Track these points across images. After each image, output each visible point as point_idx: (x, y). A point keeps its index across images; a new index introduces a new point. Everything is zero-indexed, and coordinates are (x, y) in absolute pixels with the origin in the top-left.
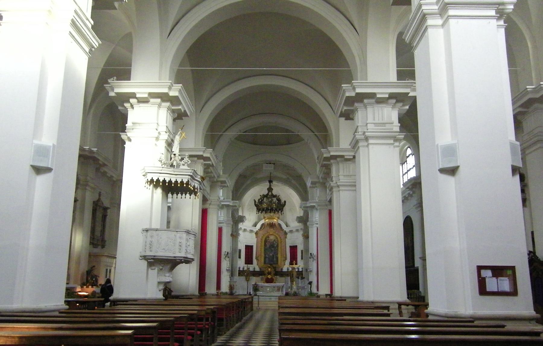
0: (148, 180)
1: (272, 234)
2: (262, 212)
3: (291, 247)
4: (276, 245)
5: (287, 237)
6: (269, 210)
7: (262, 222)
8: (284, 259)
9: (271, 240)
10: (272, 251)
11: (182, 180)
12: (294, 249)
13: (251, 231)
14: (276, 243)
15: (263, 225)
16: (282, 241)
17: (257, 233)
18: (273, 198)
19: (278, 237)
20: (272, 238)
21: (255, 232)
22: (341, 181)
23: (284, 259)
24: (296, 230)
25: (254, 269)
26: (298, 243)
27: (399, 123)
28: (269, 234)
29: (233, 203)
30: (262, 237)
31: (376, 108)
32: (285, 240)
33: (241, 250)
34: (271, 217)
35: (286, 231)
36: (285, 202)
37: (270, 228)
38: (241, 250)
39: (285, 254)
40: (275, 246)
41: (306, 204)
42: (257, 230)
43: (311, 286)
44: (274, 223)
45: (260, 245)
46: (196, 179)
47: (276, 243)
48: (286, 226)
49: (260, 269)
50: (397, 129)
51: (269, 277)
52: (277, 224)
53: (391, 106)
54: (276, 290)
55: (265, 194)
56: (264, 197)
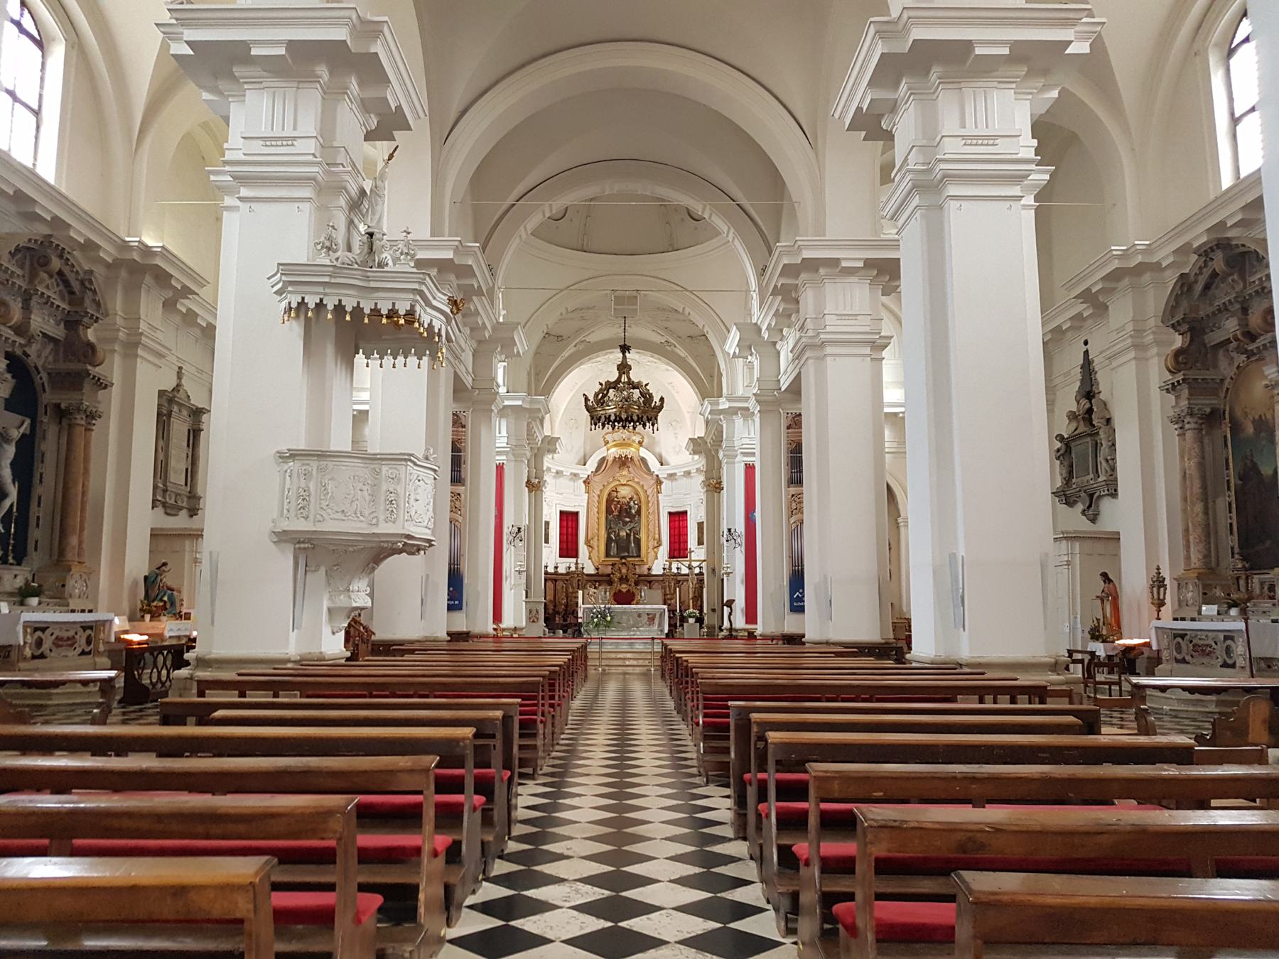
0: (290, 303)
1: (625, 482)
2: (604, 425)
3: (670, 513)
6: (623, 420)
8: (656, 545)
9: (624, 498)
10: (625, 524)
11: (394, 304)
12: (678, 519)
15: (603, 460)
16: (649, 499)
17: (586, 482)
18: (632, 390)
20: (625, 492)
22: (828, 329)
23: (656, 545)
24: (684, 472)
27: (1033, 138)
28: (618, 483)
29: (532, 402)
30: (601, 491)
31: (968, 92)
32: (658, 497)
36: (662, 399)
39: (657, 532)
40: (633, 511)
41: (718, 404)
42: (590, 473)
43: (731, 610)
44: (629, 457)
46: (435, 303)
48: (659, 464)
49: (597, 569)
50: (1030, 154)
52: (636, 460)
53: (1014, 86)
55: (613, 380)
56: (610, 388)
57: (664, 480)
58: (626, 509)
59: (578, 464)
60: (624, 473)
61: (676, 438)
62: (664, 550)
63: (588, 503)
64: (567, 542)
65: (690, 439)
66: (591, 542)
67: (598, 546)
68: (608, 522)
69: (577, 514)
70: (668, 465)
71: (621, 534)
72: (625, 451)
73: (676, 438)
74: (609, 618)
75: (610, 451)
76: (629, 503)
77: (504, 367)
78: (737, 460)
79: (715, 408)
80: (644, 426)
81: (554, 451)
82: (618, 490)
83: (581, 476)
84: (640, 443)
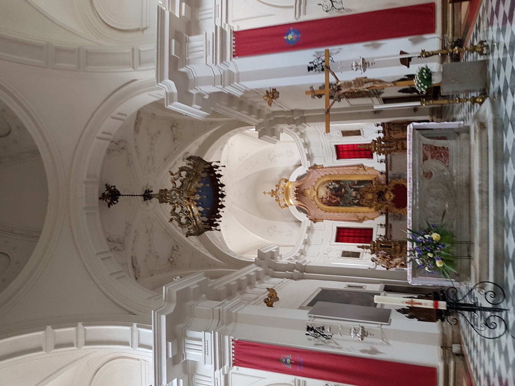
1: (315, 192)
3: (338, 158)
5: (321, 164)
8: (362, 169)
9: (327, 193)
10: (346, 192)
15: (299, 208)
16: (327, 174)
17: (315, 221)
19: (321, 181)
20: (323, 192)
21: (312, 222)
24: (305, 147)
25: (381, 225)
26: (330, 142)
28: (316, 198)
30: (322, 210)
32: (326, 168)
34: (285, 193)
35: (310, 166)
37: (305, 196)
39: (352, 168)
40: (337, 186)
42: (308, 218)
45: (336, 214)
47: (332, 184)
48: (301, 167)
49: (382, 213)
51: (390, 196)
52: (298, 184)
54: (442, 167)
57: (312, 165)
58: (336, 191)
59: (300, 226)
60: (309, 193)
62: (365, 162)
64: (360, 237)
65: (259, 138)
66: (360, 218)
67: (364, 213)
68: (345, 205)
69: (339, 229)
70: (300, 161)
72: (291, 192)
74: (435, 236)
76: (331, 189)
77: (138, 326)
78: (234, 70)
80: (220, 176)
81: (272, 255)
82: (321, 197)
83: (309, 225)
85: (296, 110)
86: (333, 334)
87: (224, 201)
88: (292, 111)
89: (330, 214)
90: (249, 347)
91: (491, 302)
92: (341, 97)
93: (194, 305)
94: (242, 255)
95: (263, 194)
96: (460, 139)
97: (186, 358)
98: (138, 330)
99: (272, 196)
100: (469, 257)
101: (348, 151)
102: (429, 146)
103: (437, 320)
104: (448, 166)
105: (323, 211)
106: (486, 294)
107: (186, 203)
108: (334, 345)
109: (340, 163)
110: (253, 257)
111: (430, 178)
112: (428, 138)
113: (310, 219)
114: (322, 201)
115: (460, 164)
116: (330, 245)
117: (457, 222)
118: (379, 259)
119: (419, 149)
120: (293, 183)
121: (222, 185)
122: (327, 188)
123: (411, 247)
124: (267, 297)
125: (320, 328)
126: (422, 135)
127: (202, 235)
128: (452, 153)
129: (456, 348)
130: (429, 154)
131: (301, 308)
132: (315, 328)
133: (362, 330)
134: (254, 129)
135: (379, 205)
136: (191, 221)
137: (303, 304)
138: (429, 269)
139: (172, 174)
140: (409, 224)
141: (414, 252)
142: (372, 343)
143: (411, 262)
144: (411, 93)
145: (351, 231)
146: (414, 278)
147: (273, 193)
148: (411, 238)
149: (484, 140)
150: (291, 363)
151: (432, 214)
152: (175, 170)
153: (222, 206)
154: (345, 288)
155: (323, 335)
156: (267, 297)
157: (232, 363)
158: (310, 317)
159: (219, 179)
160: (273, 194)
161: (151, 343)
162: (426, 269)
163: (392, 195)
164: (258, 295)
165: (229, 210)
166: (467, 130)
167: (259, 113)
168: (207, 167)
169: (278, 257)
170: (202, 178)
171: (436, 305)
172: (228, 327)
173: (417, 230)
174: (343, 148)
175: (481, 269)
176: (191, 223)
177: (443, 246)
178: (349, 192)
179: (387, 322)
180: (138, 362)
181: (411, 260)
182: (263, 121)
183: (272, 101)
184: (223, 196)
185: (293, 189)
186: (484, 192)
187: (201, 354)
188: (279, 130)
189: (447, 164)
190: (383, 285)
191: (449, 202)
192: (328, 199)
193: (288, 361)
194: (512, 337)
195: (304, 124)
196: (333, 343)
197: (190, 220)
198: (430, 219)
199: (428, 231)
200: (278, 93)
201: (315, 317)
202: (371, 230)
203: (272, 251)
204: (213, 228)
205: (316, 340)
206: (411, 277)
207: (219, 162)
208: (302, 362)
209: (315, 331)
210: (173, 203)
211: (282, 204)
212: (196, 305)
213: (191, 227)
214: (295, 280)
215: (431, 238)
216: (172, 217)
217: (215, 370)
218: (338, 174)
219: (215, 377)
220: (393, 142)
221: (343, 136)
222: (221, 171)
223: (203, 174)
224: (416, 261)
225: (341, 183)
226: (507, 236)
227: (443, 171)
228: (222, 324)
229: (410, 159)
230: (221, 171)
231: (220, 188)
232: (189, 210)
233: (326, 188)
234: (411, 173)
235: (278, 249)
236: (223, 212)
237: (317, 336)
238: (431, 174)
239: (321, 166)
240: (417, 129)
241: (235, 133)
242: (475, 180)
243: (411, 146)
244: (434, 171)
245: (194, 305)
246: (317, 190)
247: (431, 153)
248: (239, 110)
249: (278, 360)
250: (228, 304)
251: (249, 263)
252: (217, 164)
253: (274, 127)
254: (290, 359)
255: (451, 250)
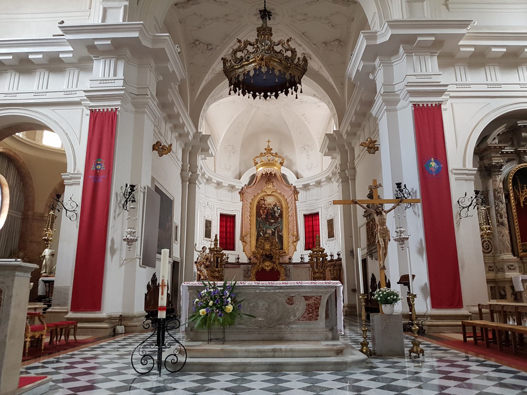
1: (270, 193)
3: (305, 216)
4: (279, 213)
5: (298, 199)
7: (252, 171)
8: (295, 240)
9: (269, 204)
13: (232, 188)
14: (278, 209)
15: (253, 177)
17: (241, 193)
19: (281, 199)
20: (270, 201)
21: (240, 190)
23: (295, 240)
25: (238, 258)
28: (265, 194)
30: (252, 200)
32: (295, 204)
33: (211, 221)
34: (269, 162)
35: (297, 187)
38: (211, 221)
39: (295, 230)
40: (277, 215)
42: (244, 186)
47: (278, 209)
48: (296, 178)
49: (250, 259)
52: (278, 175)
54: (298, 314)
57: (298, 190)
58: (272, 213)
59: (236, 178)
61: (309, 158)
62: (301, 243)
63: (242, 209)
64: (226, 238)
65: (326, 134)
66: (245, 238)
67: (250, 242)
68: (258, 223)
69: (234, 217)
71: (267, 232)
72: (270, 169)
73: (309, 158)
74: (230, 308)
75: (259, 170)
76: (273, 208)
77: (125, 6)
78: (398, 106)
79: (372, 43)
80: (287, 93)
81: (205, 150)
84: (282, 164)
85: (355, 172)
86: (128, 211)
87: (260, 98)
88: (354, 168)
89: (249, 208)
90: (110, 126)
91: (167, 360)
92: (368, 218)
93: (151, 68)
94: (204, 119)
95: (268, 140)
96: (326, 331)
97: (95, 60)
98: (122, 7)
99: (266, 149)
100: (210, 340)
101: (313, 226)
102: (320, 302)
103: (146, 312)
104: (299, 320)
105: (251, 201)
106: (175, 355)
107: (258, 57)
108: (117, 212)
109: (300, 218)
110: (203, 130)
111: (287, 303)
112: (328, 300)
113: (242, 188)
114: (261, 200)
115: (302, 331)
116: (217, 208)
117: (244, 329)
118: (205, 255)
119: (317, 292)
120: (279, 170)
121: (277, 96)
122: (275, 205)
123: (219, 285)
124: (162, 145)
125: (134, 198)
126: (331, 295)
127: (224, 75)
128: (312, 324)
129: (120, 329)
130: (311, 302)
131: (153, 179)
132: (133, 193)
133: (134, 239)
134: (335, 129)
135: (259, 256)
136: (239, 63)
137: (158, 182)
138: (197, 302)
139: (288, 41)
140: (241, 283)
141: (213, 288)
142: (121, 250)
143: (203, 285)
144: (371, 286)
145: (231, 229)
146: (187, 288)
147: (269, 150)
148: (227, 285)
149: (324, 354)
150: (97, 170)
151: (251, 305)
152: (292, 45)
153: (254, 96)
154: (175, 223)
155: (126, 201)
156: (162, 145)
157: (93, 109)
158: (145, 188)
159: (284, 93)
160: (267, 150)
161: (109, 21)
162: (197, 300)
163: (269, 268)
164: (164, 136)
165: (251, 104)
166: (335, 338)
167: (352, 134)
168: (296, 80)
169: (203, 156)
170: (285, 73)
171: (162, 309)
172: (130, 103)
173: (235, 291)
174: (316, 220)
175: (198, 351)
176: (237, 62)
177: (220, 316)
178: (270, 227)
179: (142, 265)
180: (88, 8)
181: (205, 285)
182: (344, 138)
183: (366, 147)
184: (266, 97)
185: (273, 170)
186: (274, 353)
187: (100, 76)
188: (334, 155)
189: (301, 319)
190: (179, 260)
191: (263, 321)
192: (263, 206)
193: (99, 167)
194: (135, 379)
195: (341, 181)
196: (119, 211)
197: (240, 61)
198: (246, 303)
199: (234, 301)
200: (374, 153)
201: (144, 193)
202: (233, 249)
203: (210, 150)
204: (232, 86)
205: (122, 194)
206: (188, 285)
207: (301, 92)
208: (98, 180)
209: (130, 193)
210: (257, 43)
211: (258, 160)
212: (151, 69)
213: (233, 63)
214: (181, 173)
215: (228, 304)
216: (243, 43)
217: (85, 91)
218: (289, 216)
219: (77, 92)
220: (322, 269)
221: (328, 221)
222: (292, 94)
223: (288, 74)
224: (204, 289)
225: (280, 219)
226: (231, 374)
227: (295, 316)
228: (133, 98)
229: (306, 283)
230: (292, 94)
231: (274, 94)
232: (251, 61)
233: (274, 204)
234: (293, 285)
235: (212, 155)
236: (249, 98)
237: (125, 195)
238: (292, 304)
239: (297, 198)
240: (336, 290)
241: (331, 109)
242: (285, 345)
243: (319, 285)
244: (294, 307)
245: (151, 68)
246: (272, 195)
247: (312, 304)
248: (356, 113)
249: (99, 156)
250: (153, 104)
251: (196, 127)
252: (299, 90)
253: (337, 149)
254: (101, 168)
255: (216, 323)
